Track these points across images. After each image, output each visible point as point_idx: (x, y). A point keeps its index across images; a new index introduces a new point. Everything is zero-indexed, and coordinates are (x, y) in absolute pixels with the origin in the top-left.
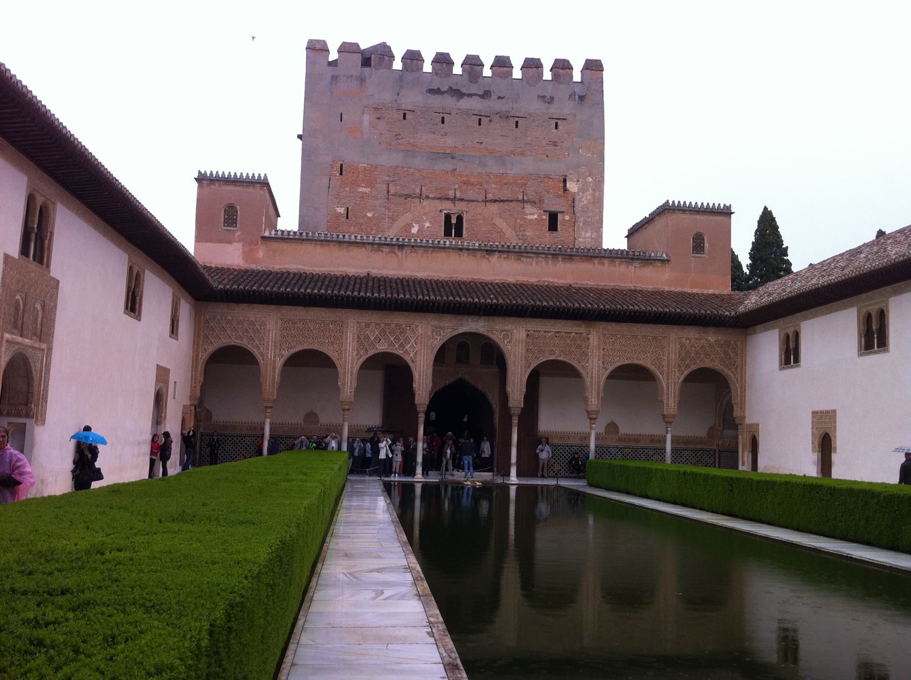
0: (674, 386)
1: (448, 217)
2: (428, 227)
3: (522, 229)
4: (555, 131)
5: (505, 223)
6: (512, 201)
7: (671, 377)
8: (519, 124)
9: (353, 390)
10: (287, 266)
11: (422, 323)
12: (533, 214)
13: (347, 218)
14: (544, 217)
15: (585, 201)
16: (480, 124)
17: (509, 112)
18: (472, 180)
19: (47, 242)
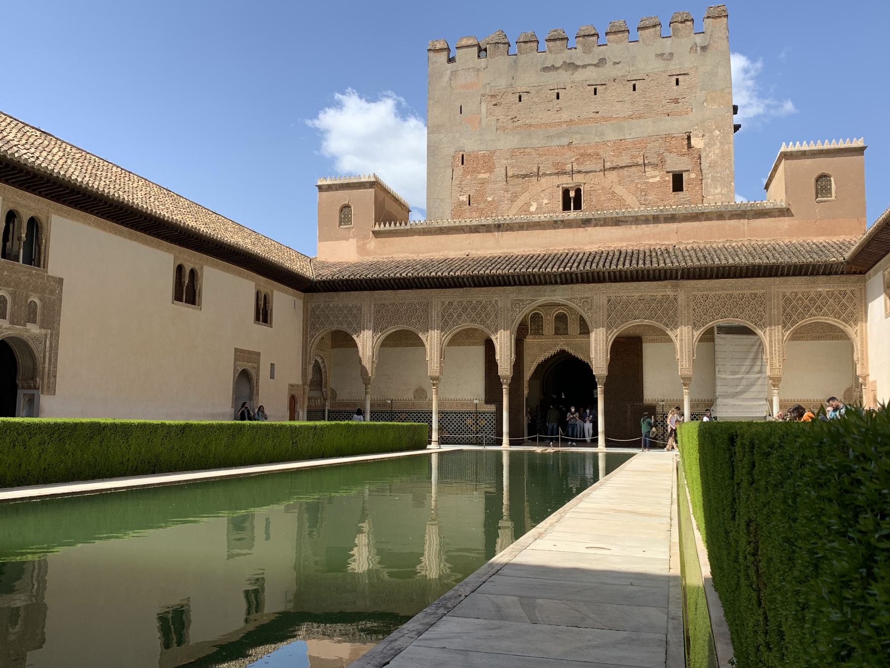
0: (779, 344)
1: (566, 192)
2: (546, 204)
3: (643, 193)
4: (676, 87)
5: (624, 190)
6: (631, 166)
7: (775, 334)
8: (636, 87)
9: (438, 365)
10: (396, 256)
11: (501, 296)
12: (655, 177)
13: (469, 205)
14: (667, 178)
15: (712, 156)
16: (595, 94)
17: (625, 76)
18: (590, 151)
19: (43, 248)
